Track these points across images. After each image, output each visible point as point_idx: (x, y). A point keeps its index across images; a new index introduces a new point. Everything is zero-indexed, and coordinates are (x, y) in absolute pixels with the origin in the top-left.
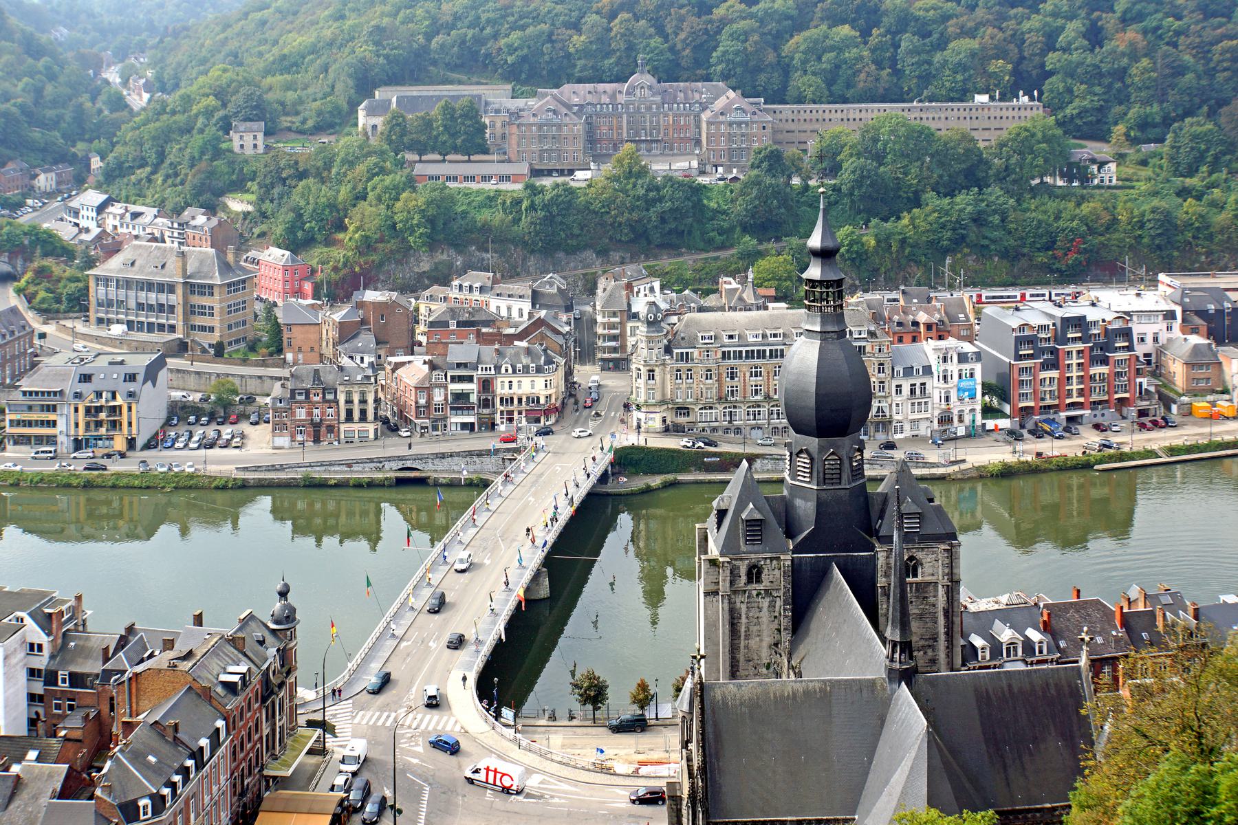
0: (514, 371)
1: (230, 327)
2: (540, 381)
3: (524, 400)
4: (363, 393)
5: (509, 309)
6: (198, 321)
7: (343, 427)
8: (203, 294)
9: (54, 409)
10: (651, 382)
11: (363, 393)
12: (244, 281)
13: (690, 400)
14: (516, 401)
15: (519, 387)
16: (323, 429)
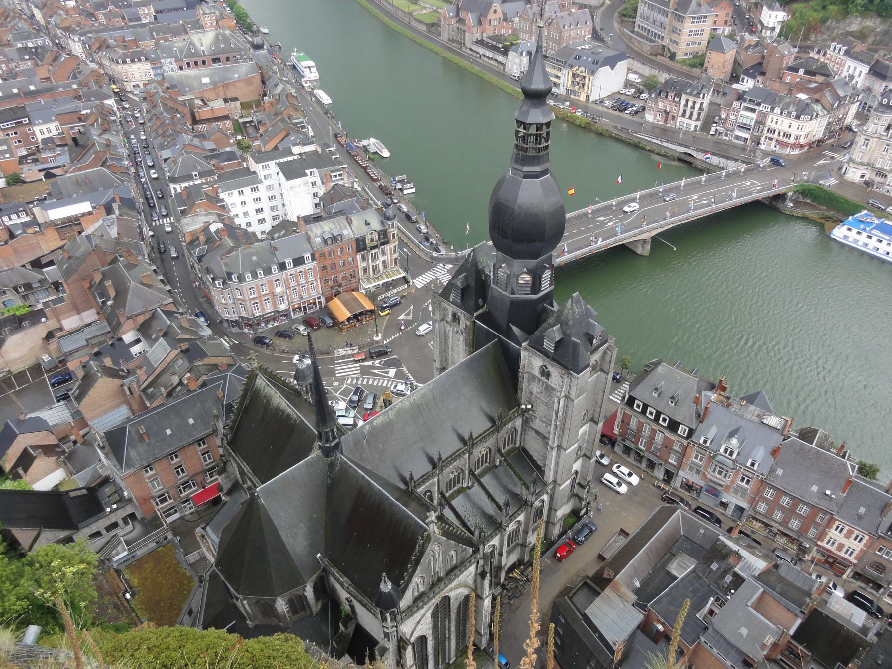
0: (781, 114)
1: (688, 44)
2: (795, 124)
3: (782, 134)
4: (694, 102)
5: (855, 69)
6: (675, 37)
7: (680, 119)
8: (679, 20)
9: (560, 70)
10: (864, 147)
11: (694, 102)
12: (705, 17)
13: (887, 168)
14: (776, 133)
15: (782, 124)
16: (670, 117)
